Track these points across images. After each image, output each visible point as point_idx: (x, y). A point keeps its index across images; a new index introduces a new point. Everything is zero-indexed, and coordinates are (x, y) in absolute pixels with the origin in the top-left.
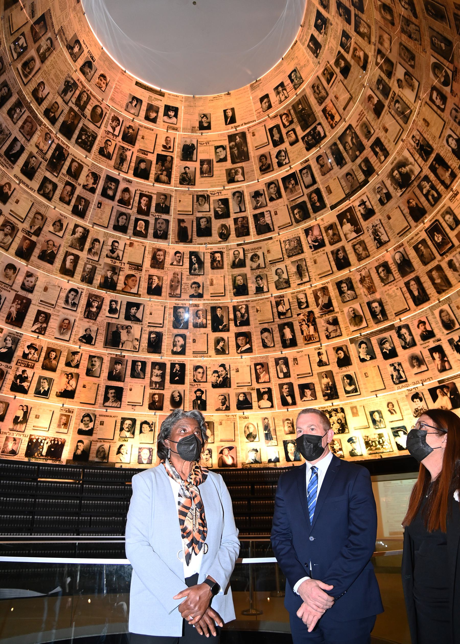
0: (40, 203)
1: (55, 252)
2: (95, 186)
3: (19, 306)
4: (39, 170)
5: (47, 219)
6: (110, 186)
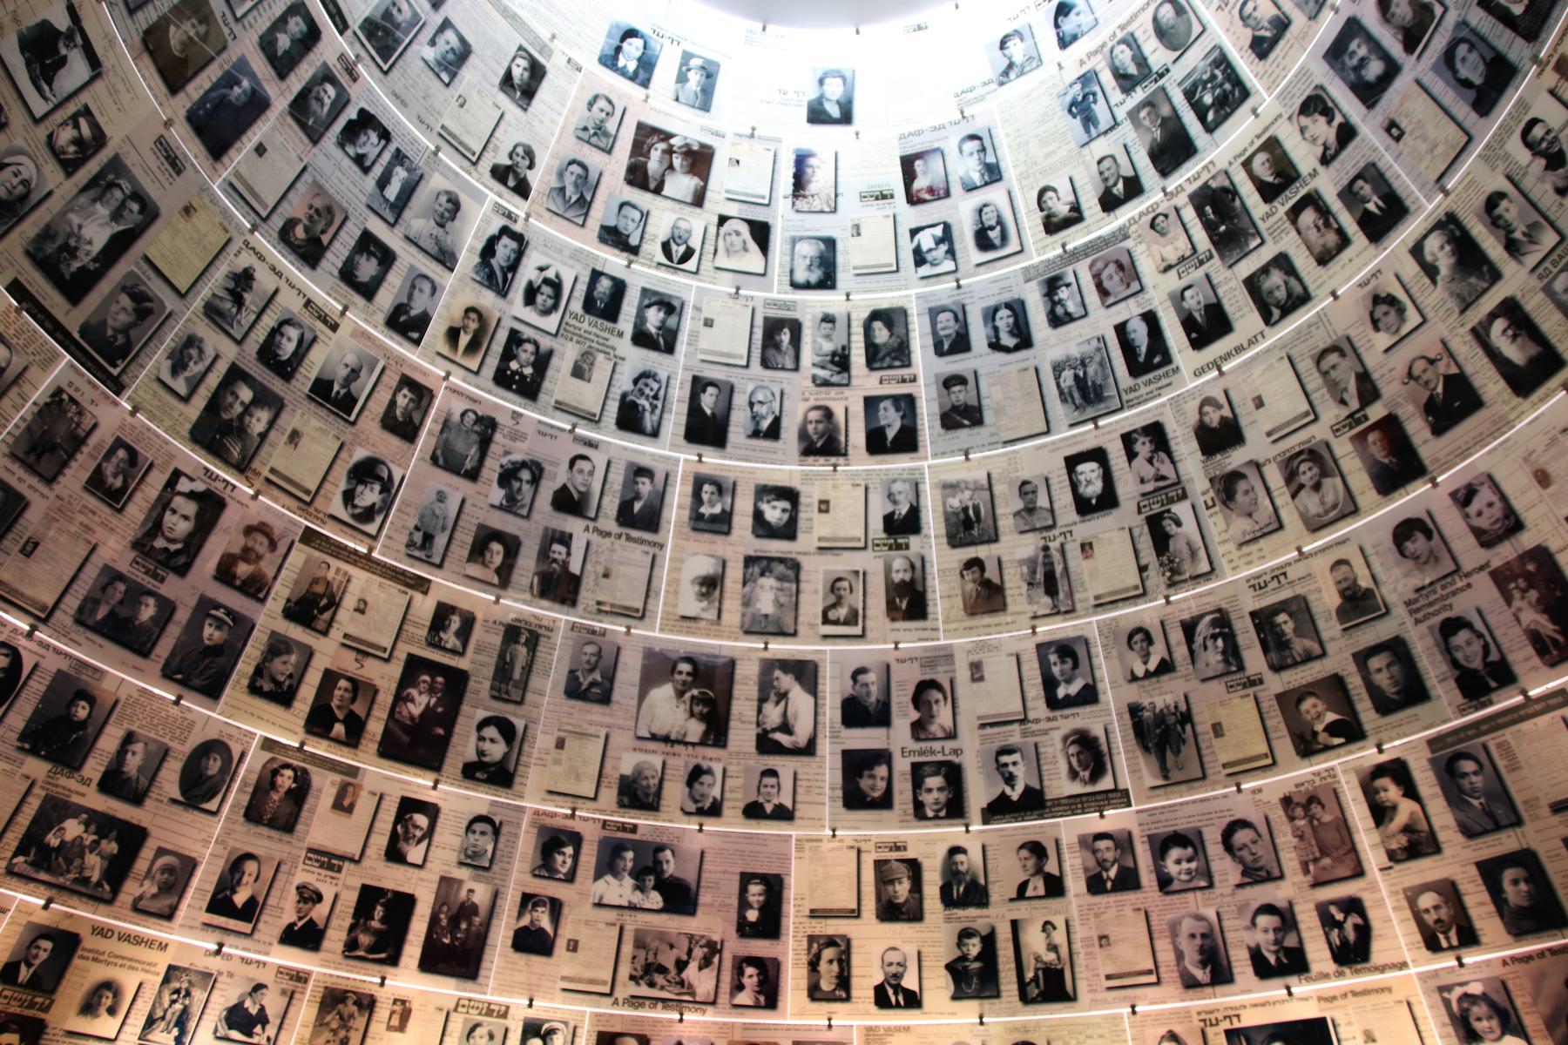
0: (1299, 335)
1: (1454, 370)
2: (1338, 119)
3: (1533, 595)
4: (1220, 292)
5: (1349, 339)
6: (1355, 61)
